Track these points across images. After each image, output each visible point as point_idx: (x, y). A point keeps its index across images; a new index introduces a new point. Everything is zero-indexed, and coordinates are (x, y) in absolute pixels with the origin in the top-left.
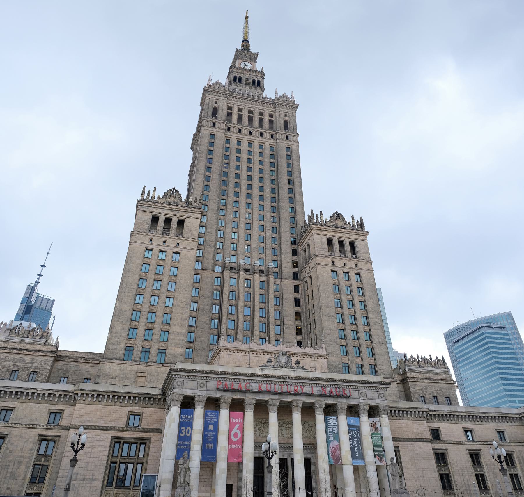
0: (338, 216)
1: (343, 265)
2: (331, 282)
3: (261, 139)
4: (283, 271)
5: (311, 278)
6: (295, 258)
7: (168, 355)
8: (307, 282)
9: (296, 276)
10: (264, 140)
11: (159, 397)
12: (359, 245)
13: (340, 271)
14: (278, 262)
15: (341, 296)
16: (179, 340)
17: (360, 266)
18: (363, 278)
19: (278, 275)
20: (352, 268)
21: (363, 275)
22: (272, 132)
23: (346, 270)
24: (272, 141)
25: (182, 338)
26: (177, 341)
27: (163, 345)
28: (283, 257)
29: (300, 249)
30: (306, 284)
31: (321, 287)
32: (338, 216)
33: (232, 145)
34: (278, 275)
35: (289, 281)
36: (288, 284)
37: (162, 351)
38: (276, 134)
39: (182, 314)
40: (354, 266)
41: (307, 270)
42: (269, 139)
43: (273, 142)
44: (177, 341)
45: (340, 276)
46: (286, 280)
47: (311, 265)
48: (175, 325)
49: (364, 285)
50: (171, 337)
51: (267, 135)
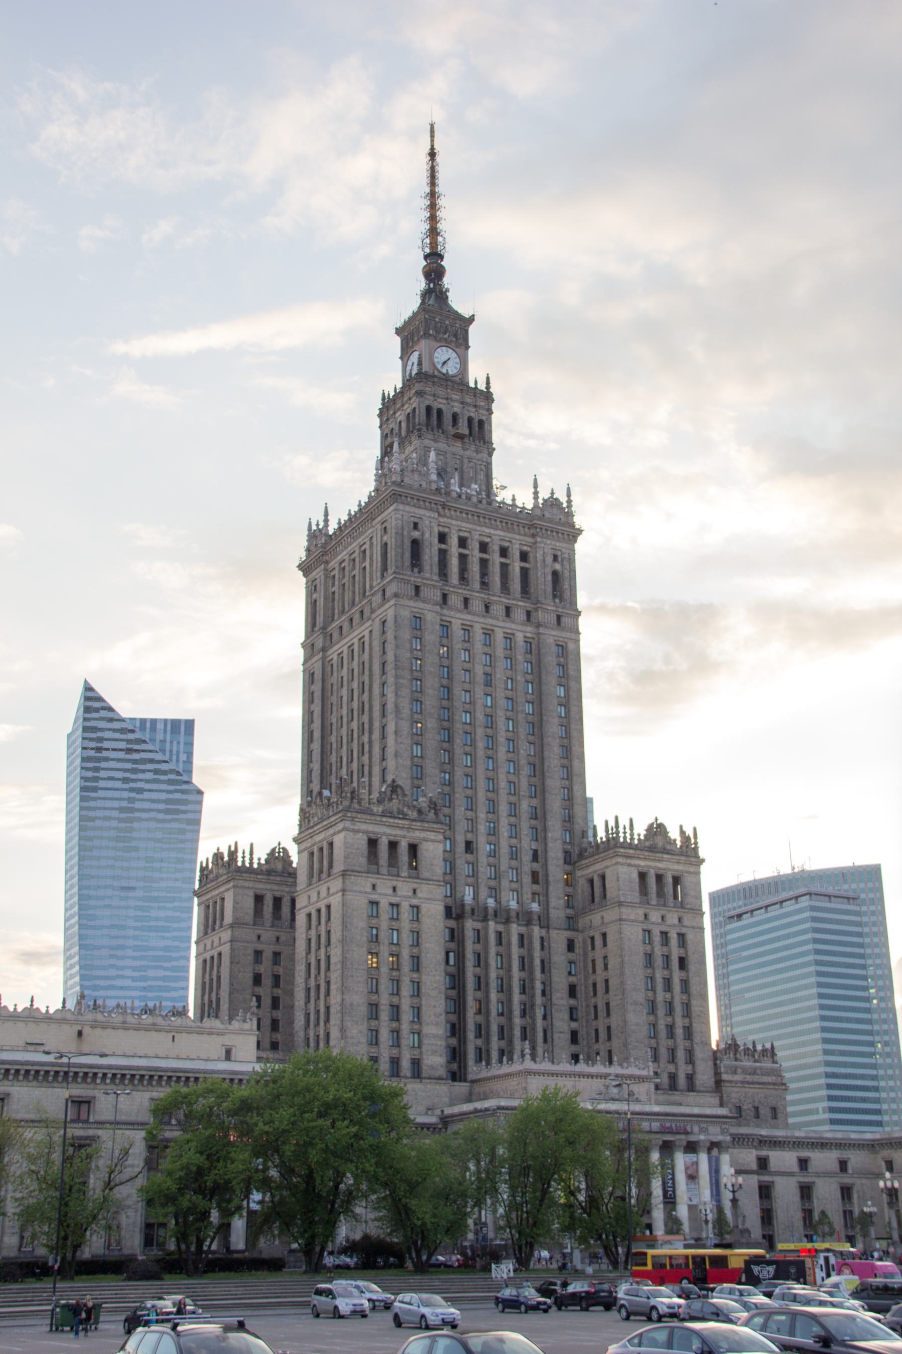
0: (657, 830)
1: (660, 920)
2: (641, 949)
3: (508, 625)
4: (551, 915)
5: (604, 935)
6: (570, 890)
7: (424, 1068)
8: (592, 938)
9: (571, 923)
10: (513, 626)
11: (440, 1126)
12: (687, 880)
13: (656, 932)
14: (543, 897)
15: (654, 973)
16: (436, 1045)
17: (686, 922)
18: (689, 942)
19: (545, 924)
20: (674, 925)
21: (690, 937)
22: (529, 606)
23: (664, 929)
24: (529, 629)
25: (439, 1043)
26: (434, 1047)
27: (415, 1053)
28: (551, 888)
29: (579, 873)
30: (589, 941)
31: (626, 958)
32: (657, 830)
33: (454, 642)
34: (545, 924)
35: (561, 932)
36: (559, 938)
37: (416, 1064)
38: (536, 610)
39: (435, 1007)
40: (676, 921)
41: (596, 918)
42: (523, 624)
43: (529, 630)
44: (434, 1047)
45: (655, 939)
46: (556, 931)
47: (610, 915)
48: (428, 1024)
49: (689, 954)
50: (426, 1041)
51: (519, 615)
